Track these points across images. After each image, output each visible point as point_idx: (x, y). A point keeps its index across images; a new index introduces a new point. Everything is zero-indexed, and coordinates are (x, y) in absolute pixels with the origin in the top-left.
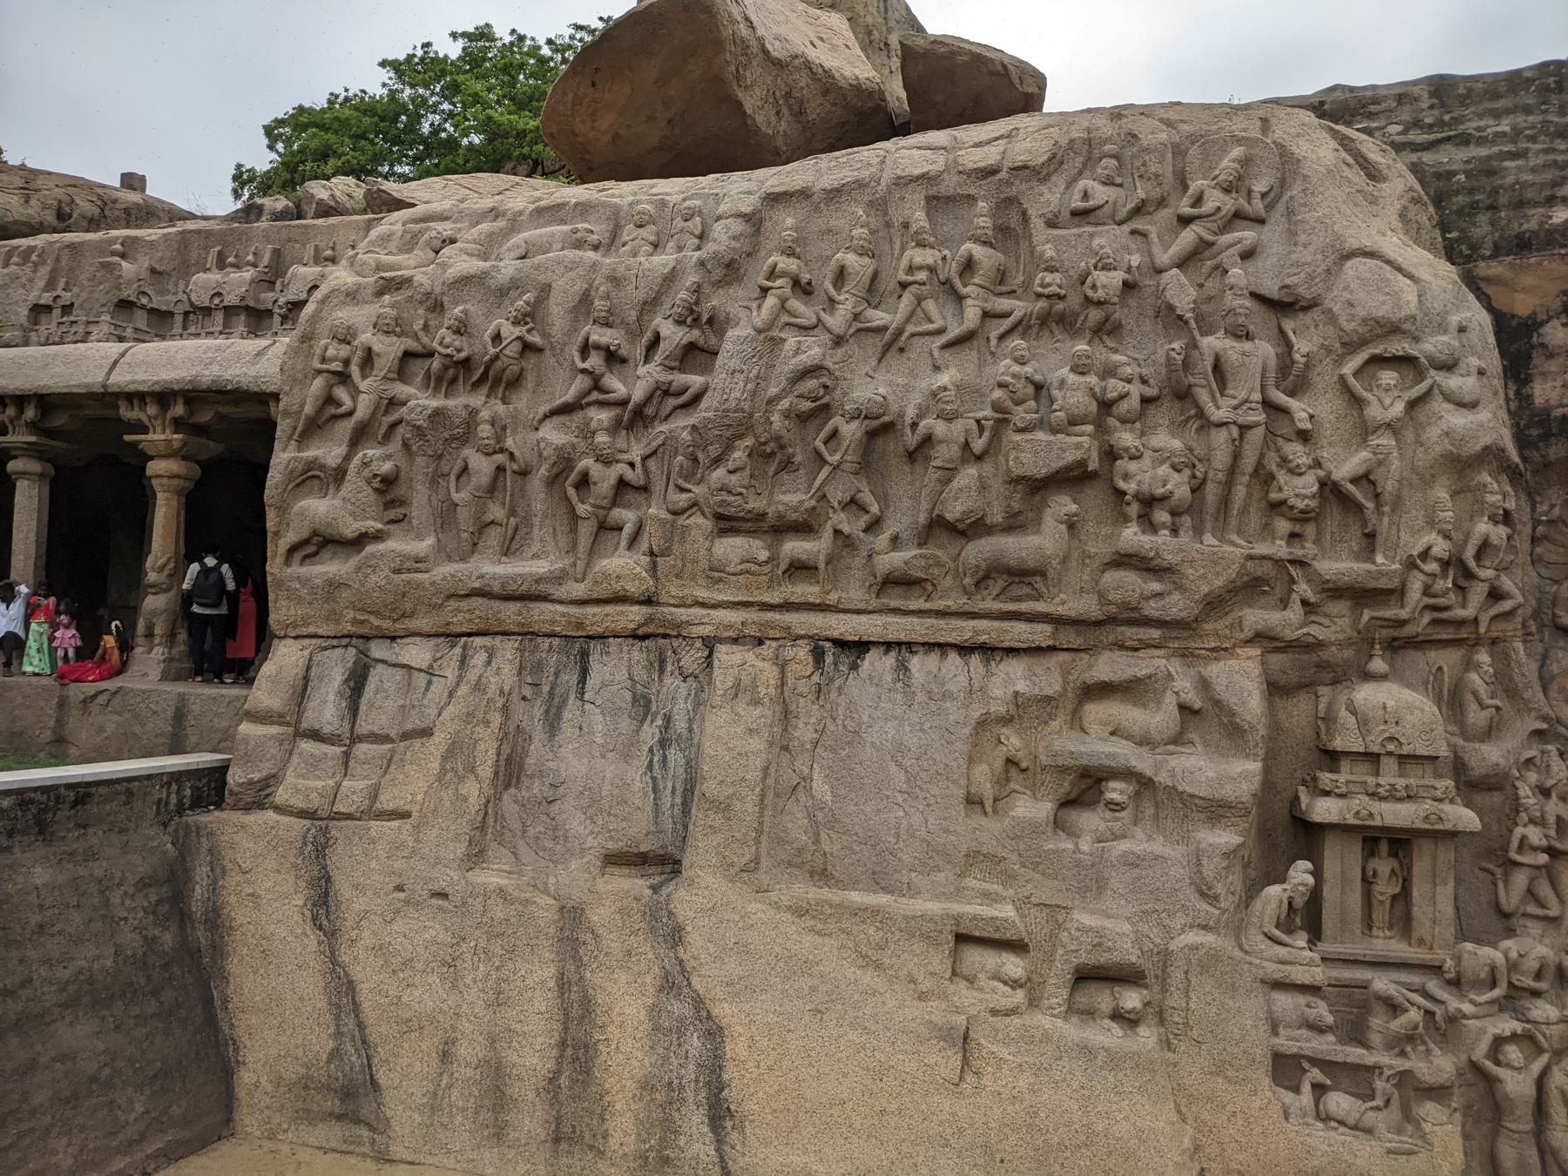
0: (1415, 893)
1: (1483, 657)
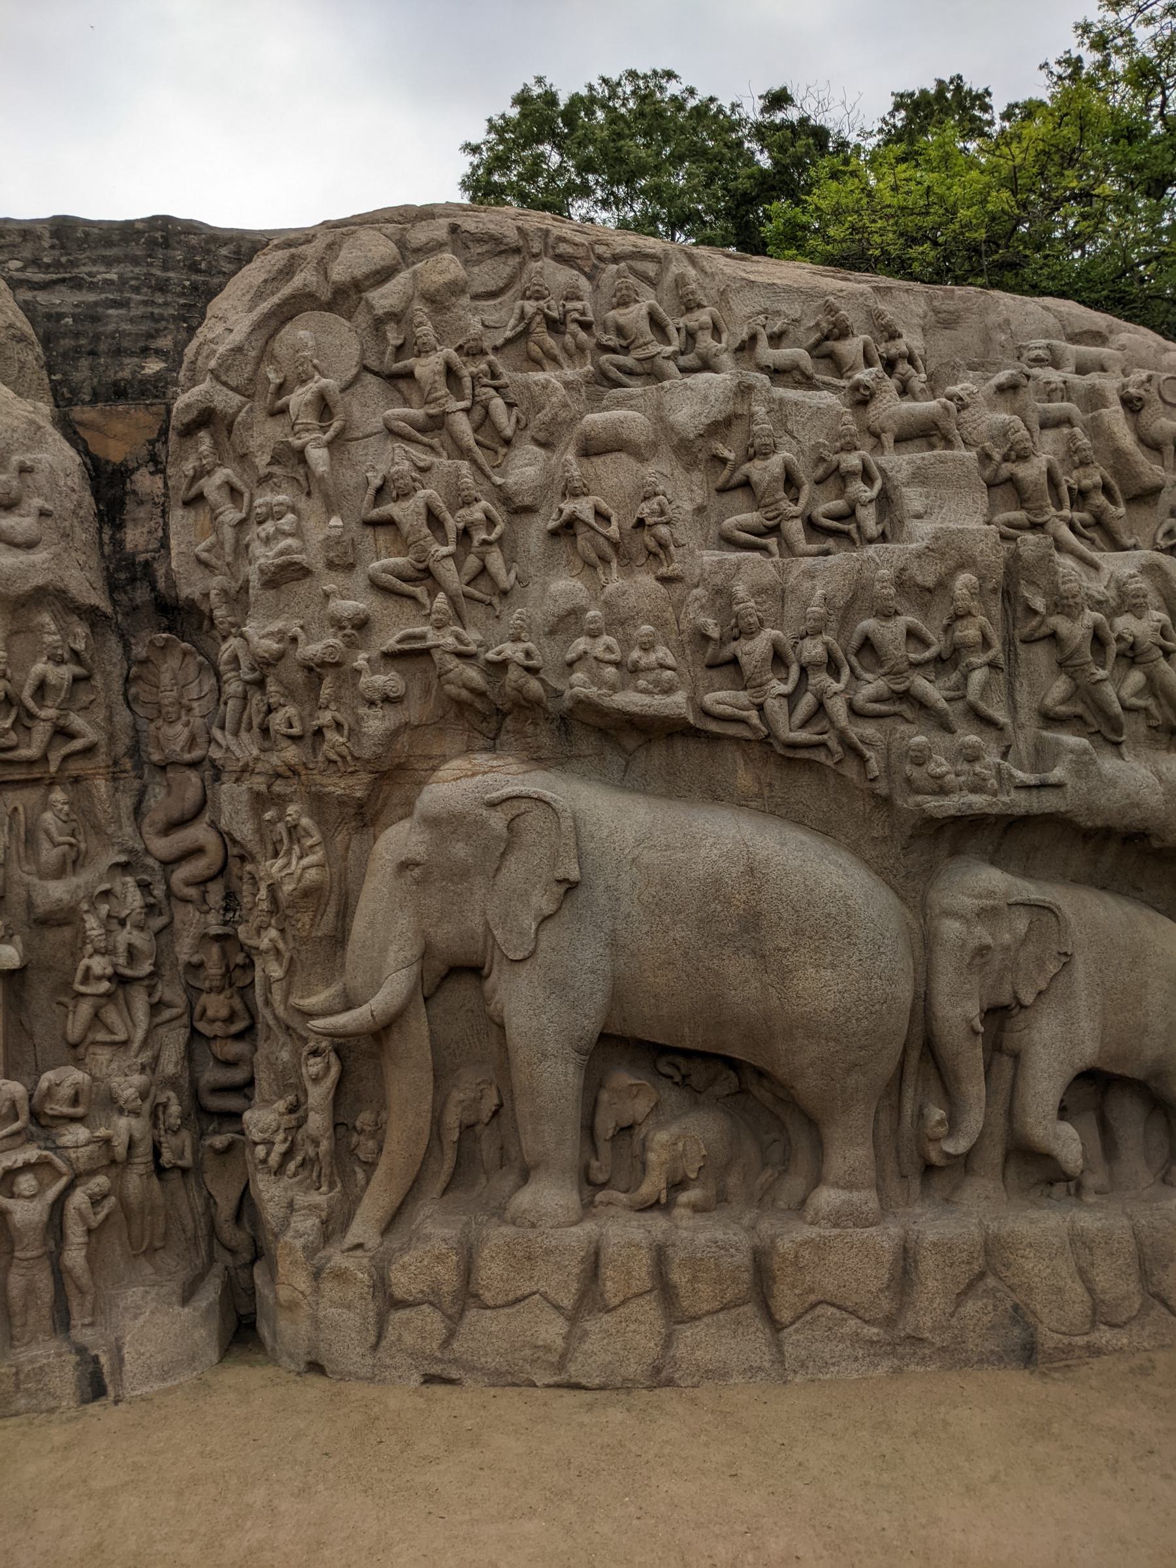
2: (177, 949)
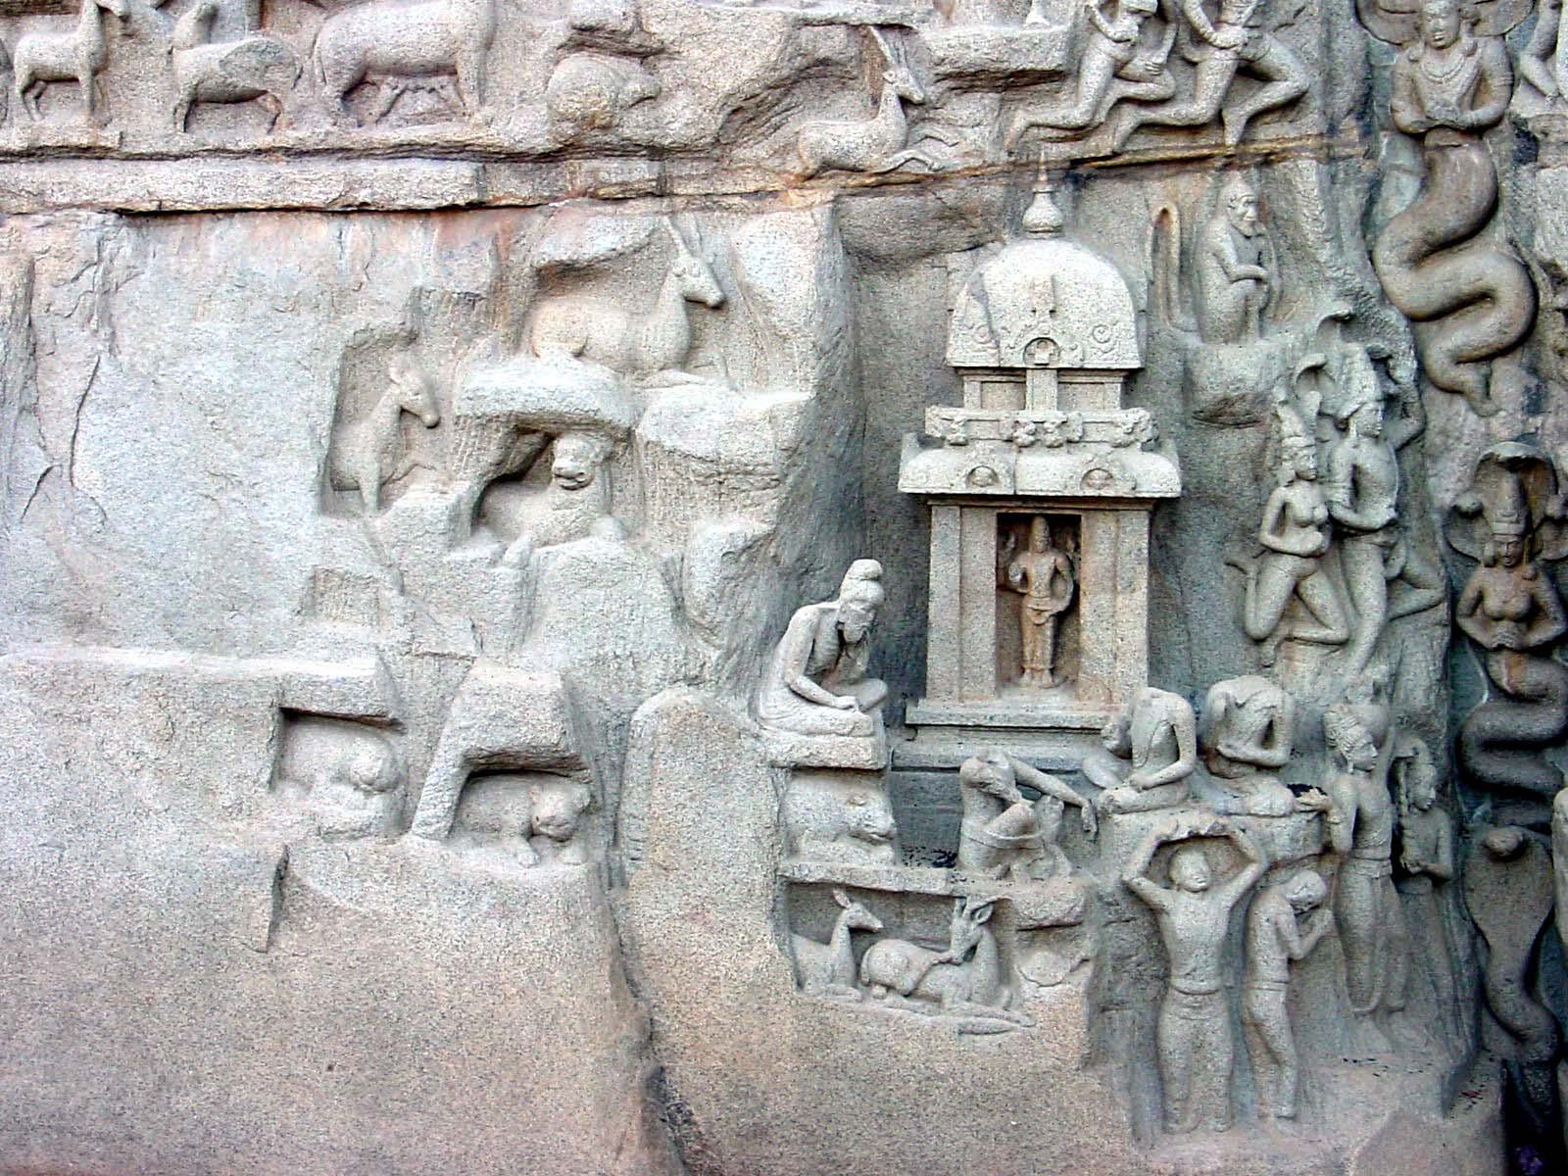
0: (1085, 607)
1: (1238, 188)
2: (1432, 481)
